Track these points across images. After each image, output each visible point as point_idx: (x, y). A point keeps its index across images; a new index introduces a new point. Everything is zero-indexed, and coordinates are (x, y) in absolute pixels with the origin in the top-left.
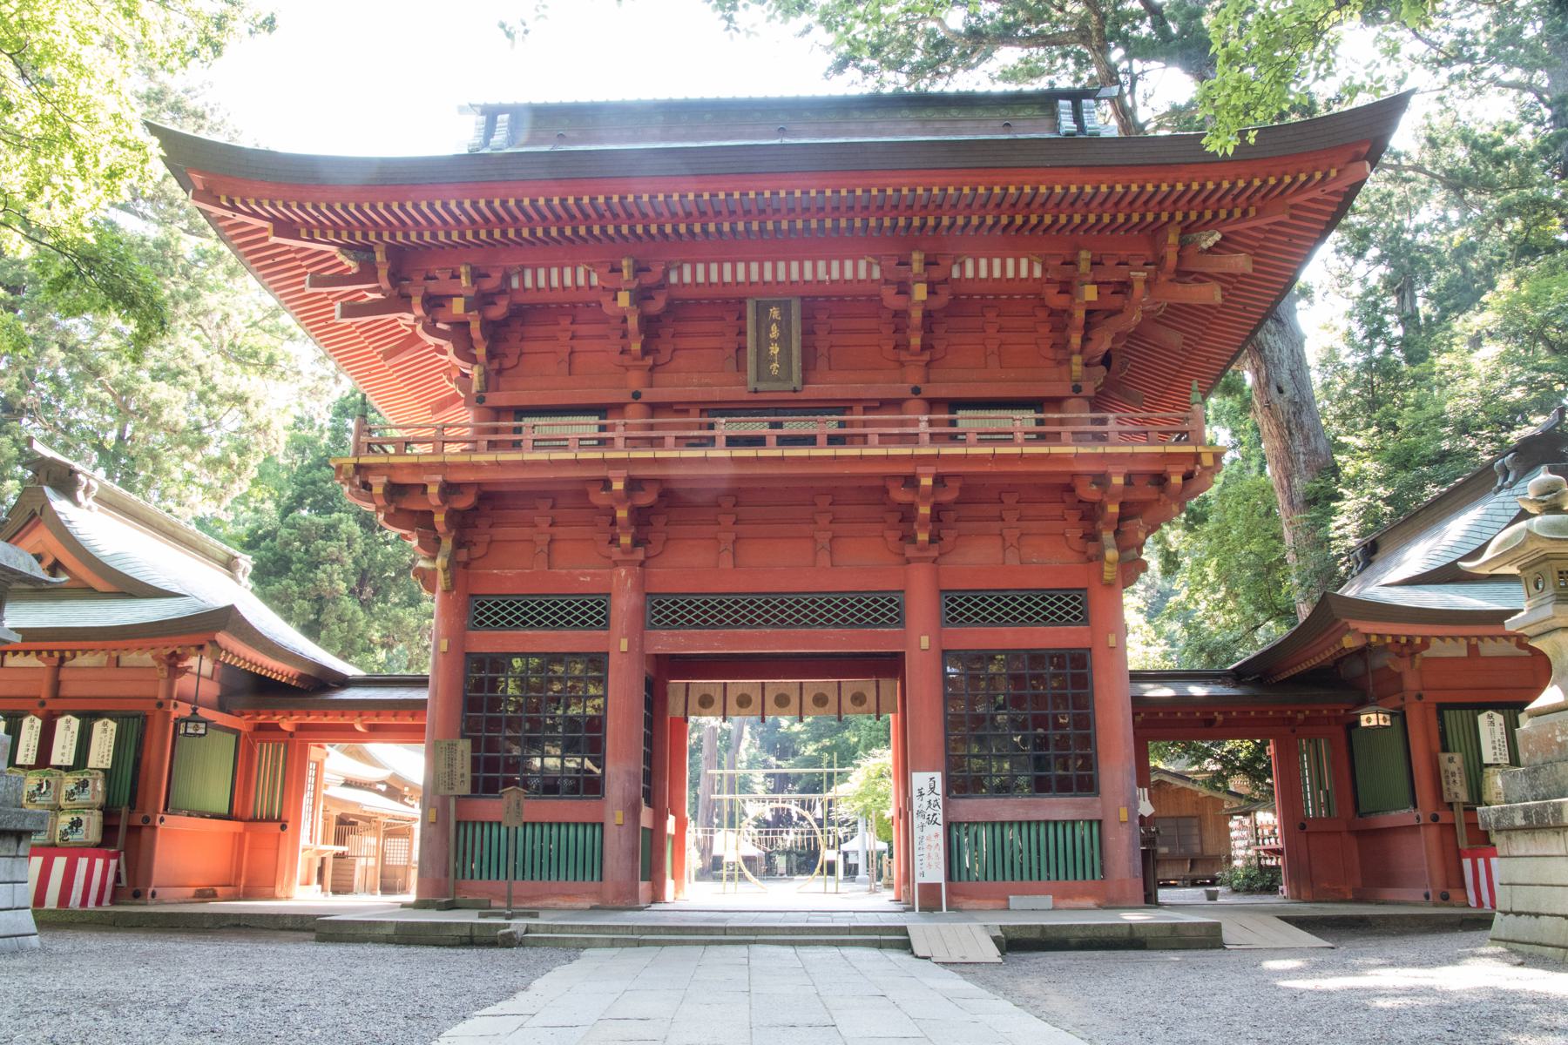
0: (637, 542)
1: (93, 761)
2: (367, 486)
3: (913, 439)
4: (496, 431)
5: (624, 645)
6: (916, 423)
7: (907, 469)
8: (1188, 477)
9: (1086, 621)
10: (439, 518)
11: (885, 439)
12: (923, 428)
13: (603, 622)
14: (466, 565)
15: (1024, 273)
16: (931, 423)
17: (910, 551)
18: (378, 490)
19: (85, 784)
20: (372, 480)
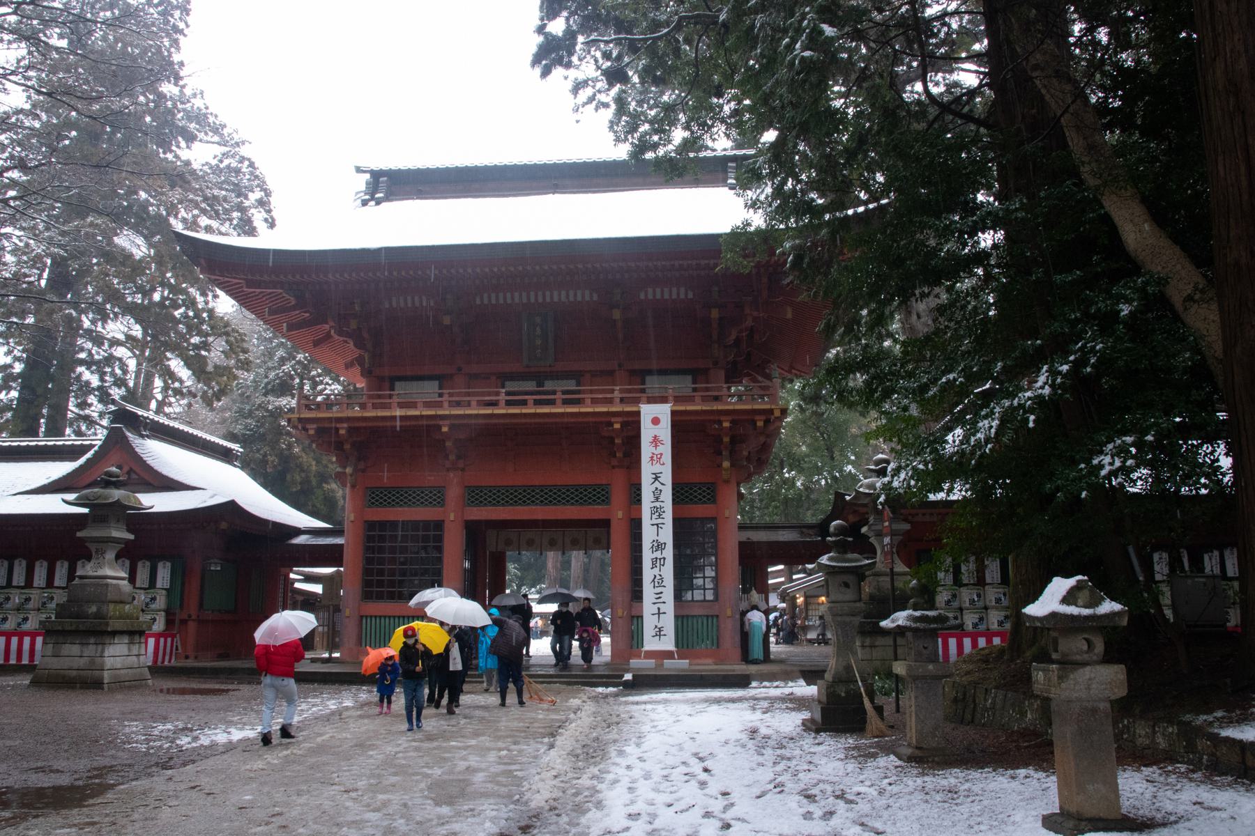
0: (459, 457)
1: (159, 585)
2: (306, 430)
3: (610, 401)
4: (379, 397)
5: (452, 517)
6: (612, 391)
7: (607, 419)
8: (767, 422)
9: (714, 502)
10: (347, 446)
11: (595, 401)
12: (617, 394)
13: (441, 503)
14: (363, 471)
15: (682, 296)
16: (621, 391)
17: (614, 462)
18: (311, 432)
19: (153, 599)
20: (308, 426)
